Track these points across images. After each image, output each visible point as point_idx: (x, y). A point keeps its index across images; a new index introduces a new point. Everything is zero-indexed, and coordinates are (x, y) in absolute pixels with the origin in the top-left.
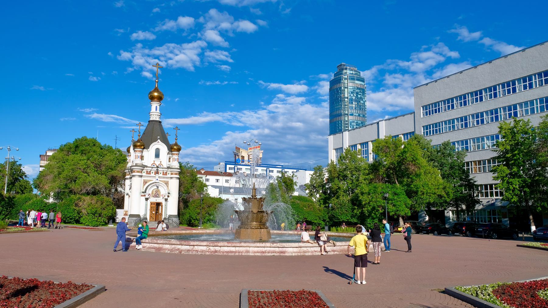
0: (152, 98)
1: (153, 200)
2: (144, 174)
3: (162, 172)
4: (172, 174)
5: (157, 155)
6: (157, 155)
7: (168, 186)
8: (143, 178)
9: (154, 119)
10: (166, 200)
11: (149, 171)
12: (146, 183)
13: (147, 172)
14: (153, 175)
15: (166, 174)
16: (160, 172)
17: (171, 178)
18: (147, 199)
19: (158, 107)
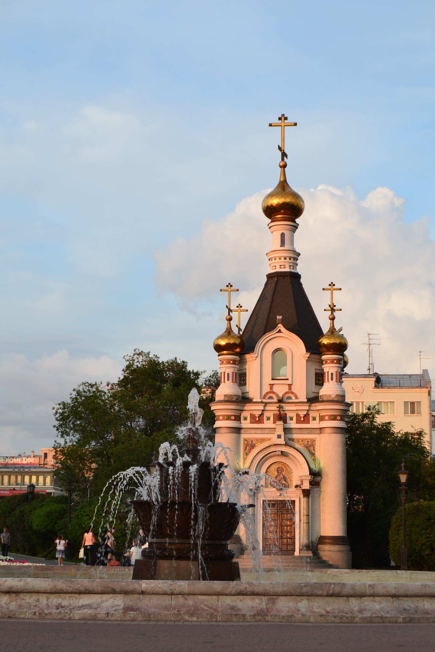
2: (246, 424)
3: (294, 415)
4: (322, 419)
9: (278, 270)
10: (306, 493)
11: (257, 414)
12: (253, 447)
13: (253, 416)
15: (306, 418)
16: (289, 415)
19: (287, 234)
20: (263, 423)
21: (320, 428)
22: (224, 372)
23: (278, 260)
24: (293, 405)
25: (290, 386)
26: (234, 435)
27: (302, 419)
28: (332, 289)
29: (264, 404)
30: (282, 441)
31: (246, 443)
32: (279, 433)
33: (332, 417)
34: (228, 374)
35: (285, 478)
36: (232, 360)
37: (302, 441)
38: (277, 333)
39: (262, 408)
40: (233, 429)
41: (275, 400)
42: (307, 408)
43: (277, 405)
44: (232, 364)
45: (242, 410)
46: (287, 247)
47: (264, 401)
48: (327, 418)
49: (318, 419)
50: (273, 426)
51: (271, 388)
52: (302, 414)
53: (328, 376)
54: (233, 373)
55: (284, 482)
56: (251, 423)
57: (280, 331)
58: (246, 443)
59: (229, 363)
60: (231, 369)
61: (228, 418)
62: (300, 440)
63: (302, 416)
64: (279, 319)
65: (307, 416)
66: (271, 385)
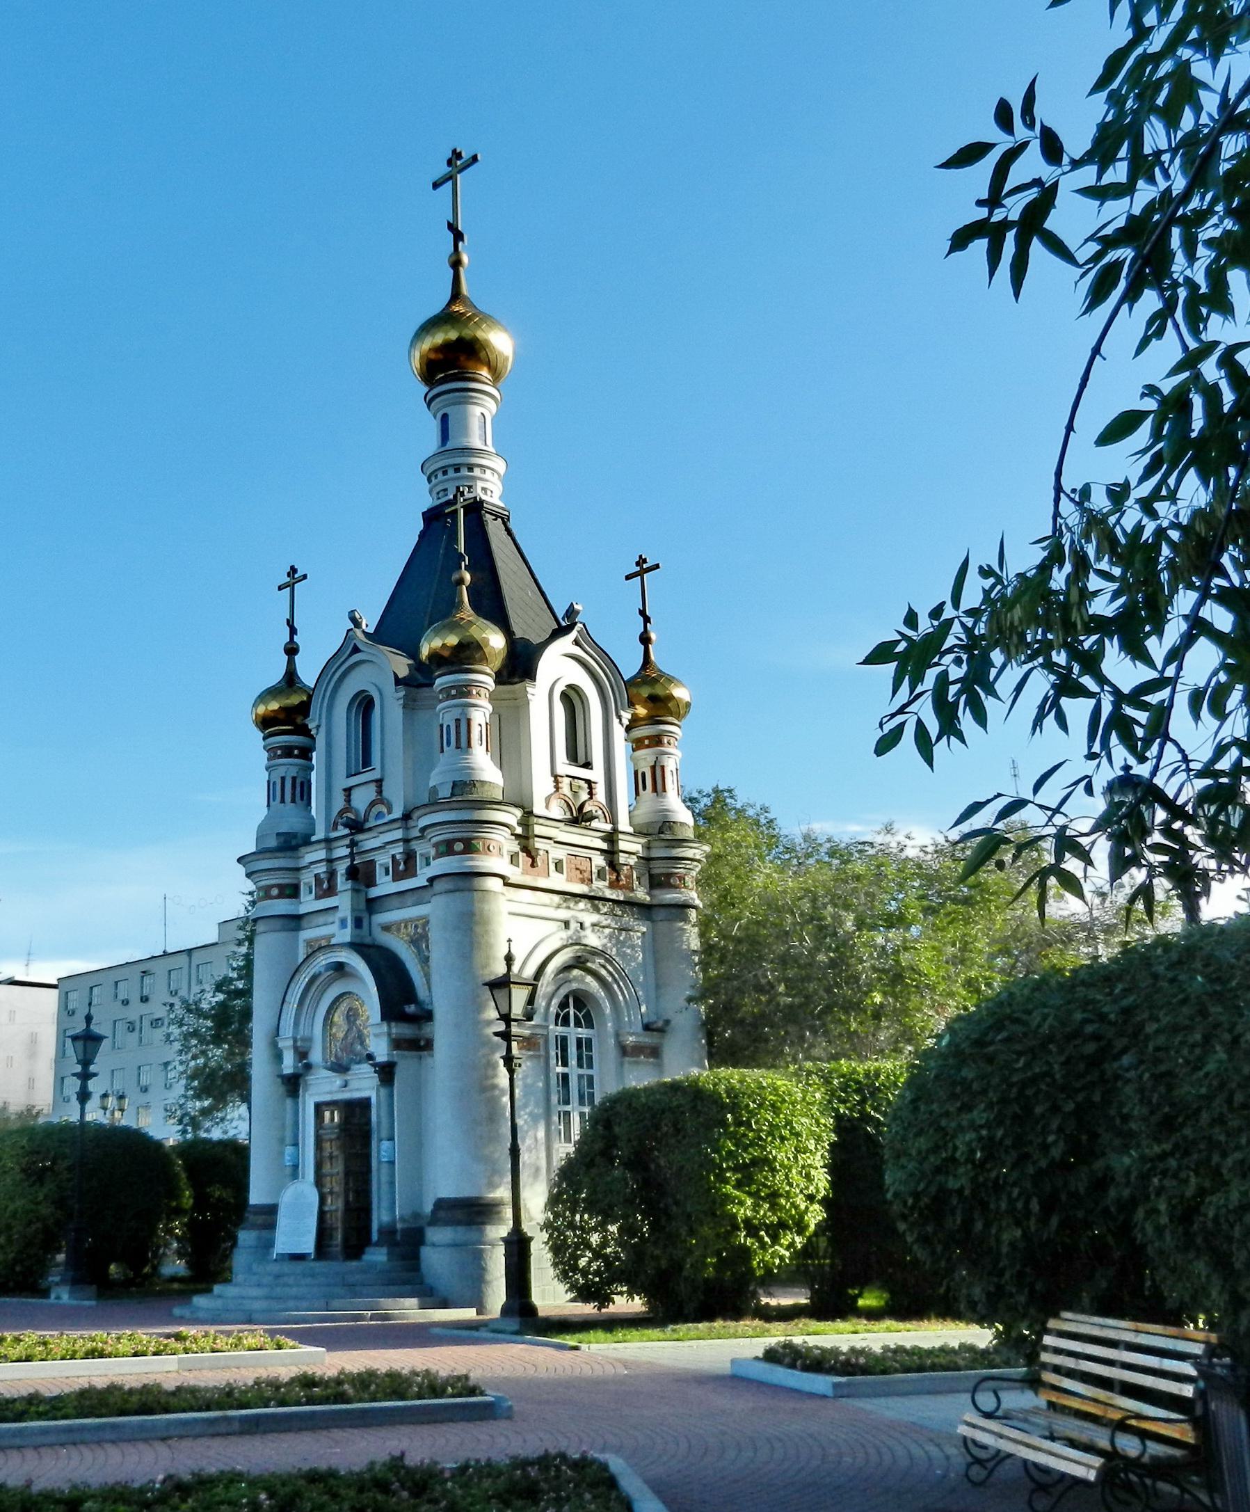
2: (308, 903)
10: (386, 1073)
25: (379, 782)
36: (297, 748)
42: (398, 834)
45: (298, 869)
51: (348, 800)
54: (283, 779)
56: (318, 898)
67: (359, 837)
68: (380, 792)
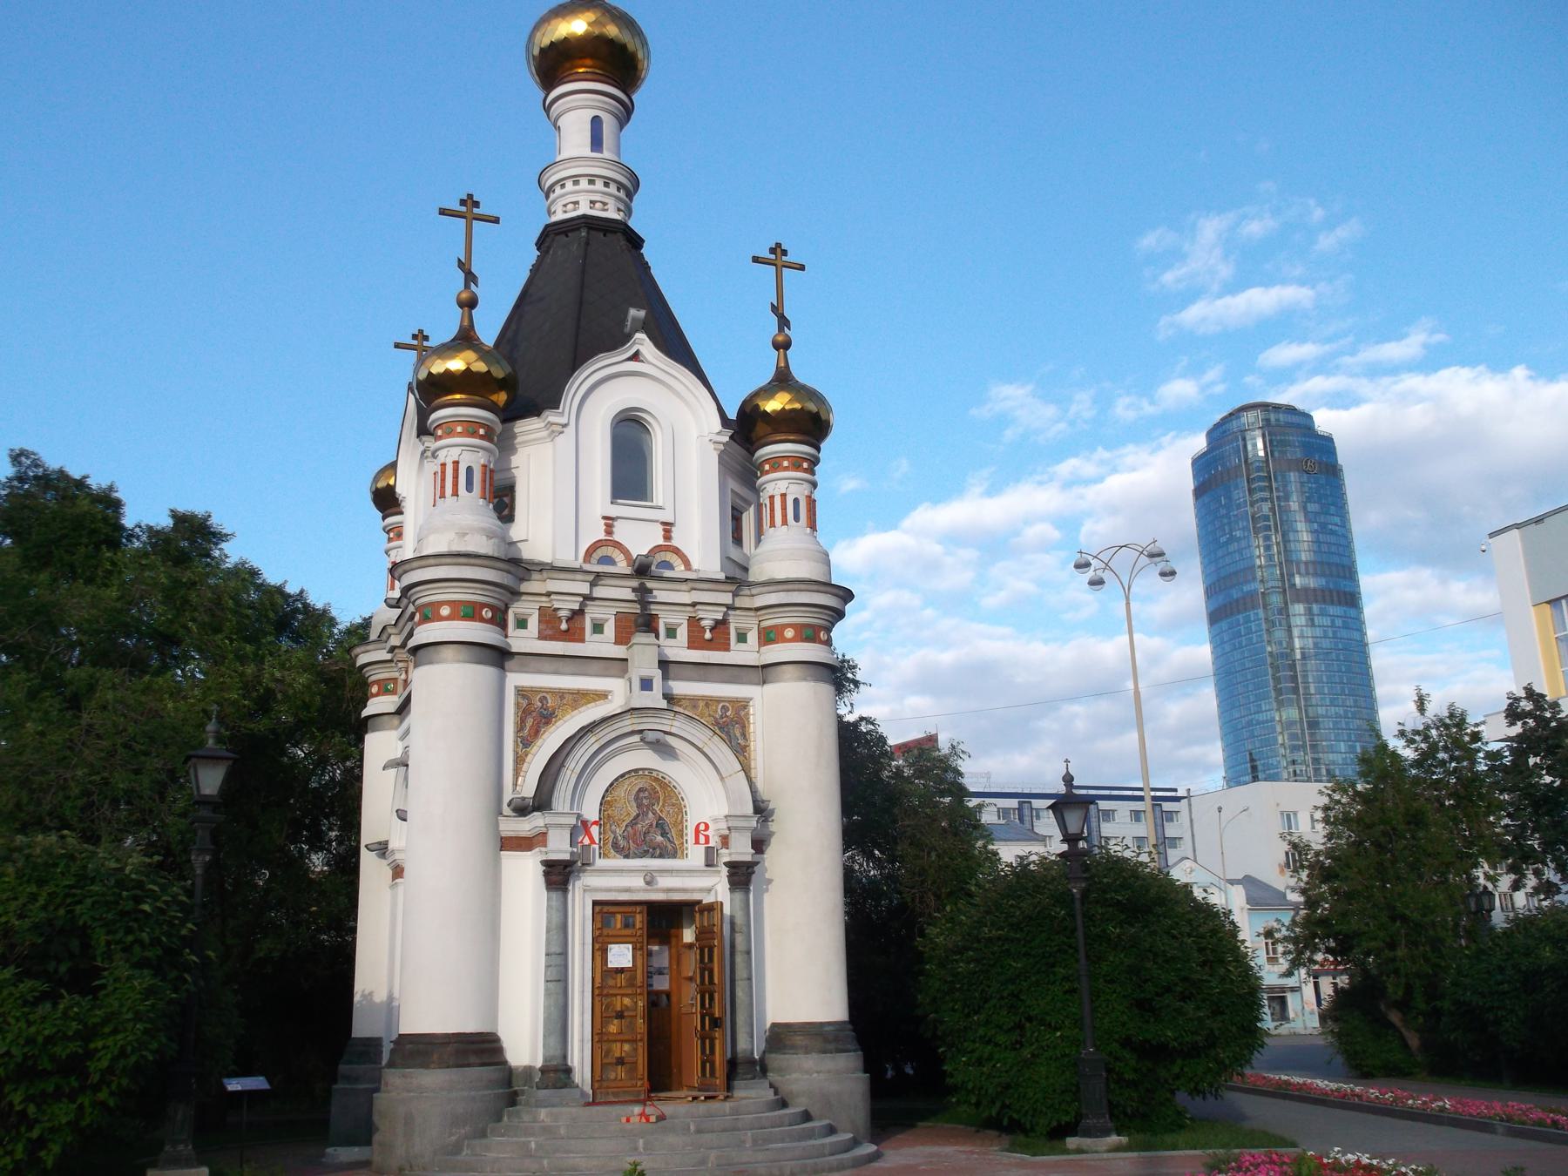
0: (554, 65)
1: (620, 878)
2: (523, 640)
3: (680, 620)
4: (769, 636)
5: (631, 472)
6: (631, 472)
7: (741, 751)
8: (517, 679)
9: (584, 209)
10: (741, 876)
11: (566, 606)
13: (548, 619)
14: (602, 645)
15: (719, 635)
16: (665, 618)
17: (764, 673)
18: (558, 875)
19: (609, 123)
20: (583, 641)
21: (764, 667)
22: (456, 463)
23: (584, 183)
24: (684, 587)
25: (668, 527)
26: (487, 672)
27: (708, 635)
28: (779, 263)
29: (591, 578)
30: (655, 699)
31: (524, 703)
32: (646, 673)
33: (809, 632)
34: (469, 470)
35: (661, 826)
37: (707, 705)
38: (629, 359)
39: (584, 589)
40: (488, 651)
41: (622, 566)
43: (635, 583)
44: (482, 437)
46: (606, 154)
47: (587, 567)
48: (789, 633)
49: (752, 637)
50: (619, 651)
51: (609, 531)
52: (709, 617)
53: (784, 508)
54: (484, 466)
55: (659, 838)
56: (542, 637)
57: (636, 357)
58: (524, 703)
59: (474, 434)
60: (482, 453)
61: (470, 612)
62: (701, 704)
63: (707, 623)
64: (634, 319)
65: (720, 625)
66: (609, 522)
67: (650, 584)
68: (667, 535)
